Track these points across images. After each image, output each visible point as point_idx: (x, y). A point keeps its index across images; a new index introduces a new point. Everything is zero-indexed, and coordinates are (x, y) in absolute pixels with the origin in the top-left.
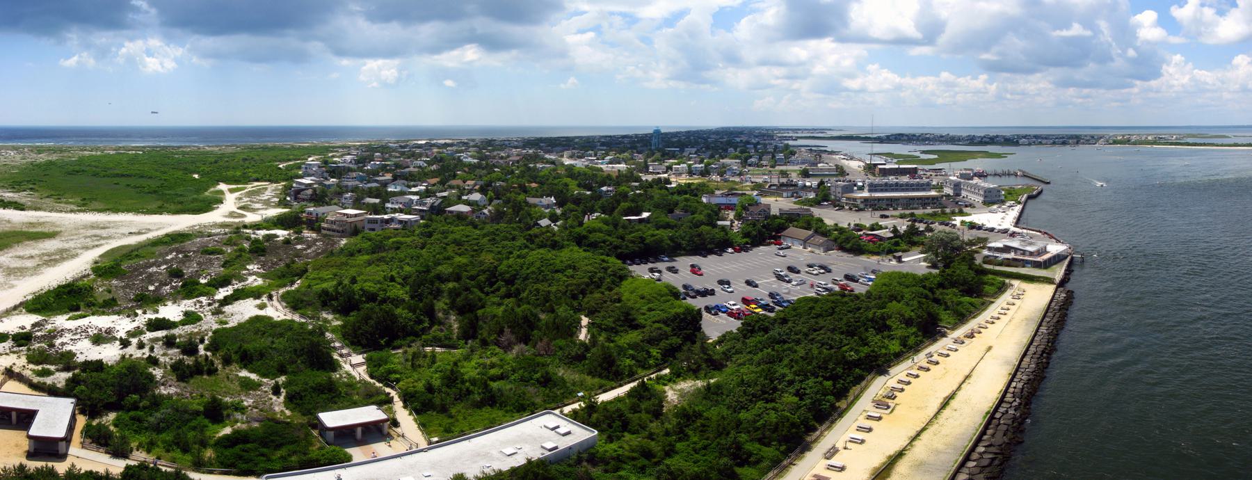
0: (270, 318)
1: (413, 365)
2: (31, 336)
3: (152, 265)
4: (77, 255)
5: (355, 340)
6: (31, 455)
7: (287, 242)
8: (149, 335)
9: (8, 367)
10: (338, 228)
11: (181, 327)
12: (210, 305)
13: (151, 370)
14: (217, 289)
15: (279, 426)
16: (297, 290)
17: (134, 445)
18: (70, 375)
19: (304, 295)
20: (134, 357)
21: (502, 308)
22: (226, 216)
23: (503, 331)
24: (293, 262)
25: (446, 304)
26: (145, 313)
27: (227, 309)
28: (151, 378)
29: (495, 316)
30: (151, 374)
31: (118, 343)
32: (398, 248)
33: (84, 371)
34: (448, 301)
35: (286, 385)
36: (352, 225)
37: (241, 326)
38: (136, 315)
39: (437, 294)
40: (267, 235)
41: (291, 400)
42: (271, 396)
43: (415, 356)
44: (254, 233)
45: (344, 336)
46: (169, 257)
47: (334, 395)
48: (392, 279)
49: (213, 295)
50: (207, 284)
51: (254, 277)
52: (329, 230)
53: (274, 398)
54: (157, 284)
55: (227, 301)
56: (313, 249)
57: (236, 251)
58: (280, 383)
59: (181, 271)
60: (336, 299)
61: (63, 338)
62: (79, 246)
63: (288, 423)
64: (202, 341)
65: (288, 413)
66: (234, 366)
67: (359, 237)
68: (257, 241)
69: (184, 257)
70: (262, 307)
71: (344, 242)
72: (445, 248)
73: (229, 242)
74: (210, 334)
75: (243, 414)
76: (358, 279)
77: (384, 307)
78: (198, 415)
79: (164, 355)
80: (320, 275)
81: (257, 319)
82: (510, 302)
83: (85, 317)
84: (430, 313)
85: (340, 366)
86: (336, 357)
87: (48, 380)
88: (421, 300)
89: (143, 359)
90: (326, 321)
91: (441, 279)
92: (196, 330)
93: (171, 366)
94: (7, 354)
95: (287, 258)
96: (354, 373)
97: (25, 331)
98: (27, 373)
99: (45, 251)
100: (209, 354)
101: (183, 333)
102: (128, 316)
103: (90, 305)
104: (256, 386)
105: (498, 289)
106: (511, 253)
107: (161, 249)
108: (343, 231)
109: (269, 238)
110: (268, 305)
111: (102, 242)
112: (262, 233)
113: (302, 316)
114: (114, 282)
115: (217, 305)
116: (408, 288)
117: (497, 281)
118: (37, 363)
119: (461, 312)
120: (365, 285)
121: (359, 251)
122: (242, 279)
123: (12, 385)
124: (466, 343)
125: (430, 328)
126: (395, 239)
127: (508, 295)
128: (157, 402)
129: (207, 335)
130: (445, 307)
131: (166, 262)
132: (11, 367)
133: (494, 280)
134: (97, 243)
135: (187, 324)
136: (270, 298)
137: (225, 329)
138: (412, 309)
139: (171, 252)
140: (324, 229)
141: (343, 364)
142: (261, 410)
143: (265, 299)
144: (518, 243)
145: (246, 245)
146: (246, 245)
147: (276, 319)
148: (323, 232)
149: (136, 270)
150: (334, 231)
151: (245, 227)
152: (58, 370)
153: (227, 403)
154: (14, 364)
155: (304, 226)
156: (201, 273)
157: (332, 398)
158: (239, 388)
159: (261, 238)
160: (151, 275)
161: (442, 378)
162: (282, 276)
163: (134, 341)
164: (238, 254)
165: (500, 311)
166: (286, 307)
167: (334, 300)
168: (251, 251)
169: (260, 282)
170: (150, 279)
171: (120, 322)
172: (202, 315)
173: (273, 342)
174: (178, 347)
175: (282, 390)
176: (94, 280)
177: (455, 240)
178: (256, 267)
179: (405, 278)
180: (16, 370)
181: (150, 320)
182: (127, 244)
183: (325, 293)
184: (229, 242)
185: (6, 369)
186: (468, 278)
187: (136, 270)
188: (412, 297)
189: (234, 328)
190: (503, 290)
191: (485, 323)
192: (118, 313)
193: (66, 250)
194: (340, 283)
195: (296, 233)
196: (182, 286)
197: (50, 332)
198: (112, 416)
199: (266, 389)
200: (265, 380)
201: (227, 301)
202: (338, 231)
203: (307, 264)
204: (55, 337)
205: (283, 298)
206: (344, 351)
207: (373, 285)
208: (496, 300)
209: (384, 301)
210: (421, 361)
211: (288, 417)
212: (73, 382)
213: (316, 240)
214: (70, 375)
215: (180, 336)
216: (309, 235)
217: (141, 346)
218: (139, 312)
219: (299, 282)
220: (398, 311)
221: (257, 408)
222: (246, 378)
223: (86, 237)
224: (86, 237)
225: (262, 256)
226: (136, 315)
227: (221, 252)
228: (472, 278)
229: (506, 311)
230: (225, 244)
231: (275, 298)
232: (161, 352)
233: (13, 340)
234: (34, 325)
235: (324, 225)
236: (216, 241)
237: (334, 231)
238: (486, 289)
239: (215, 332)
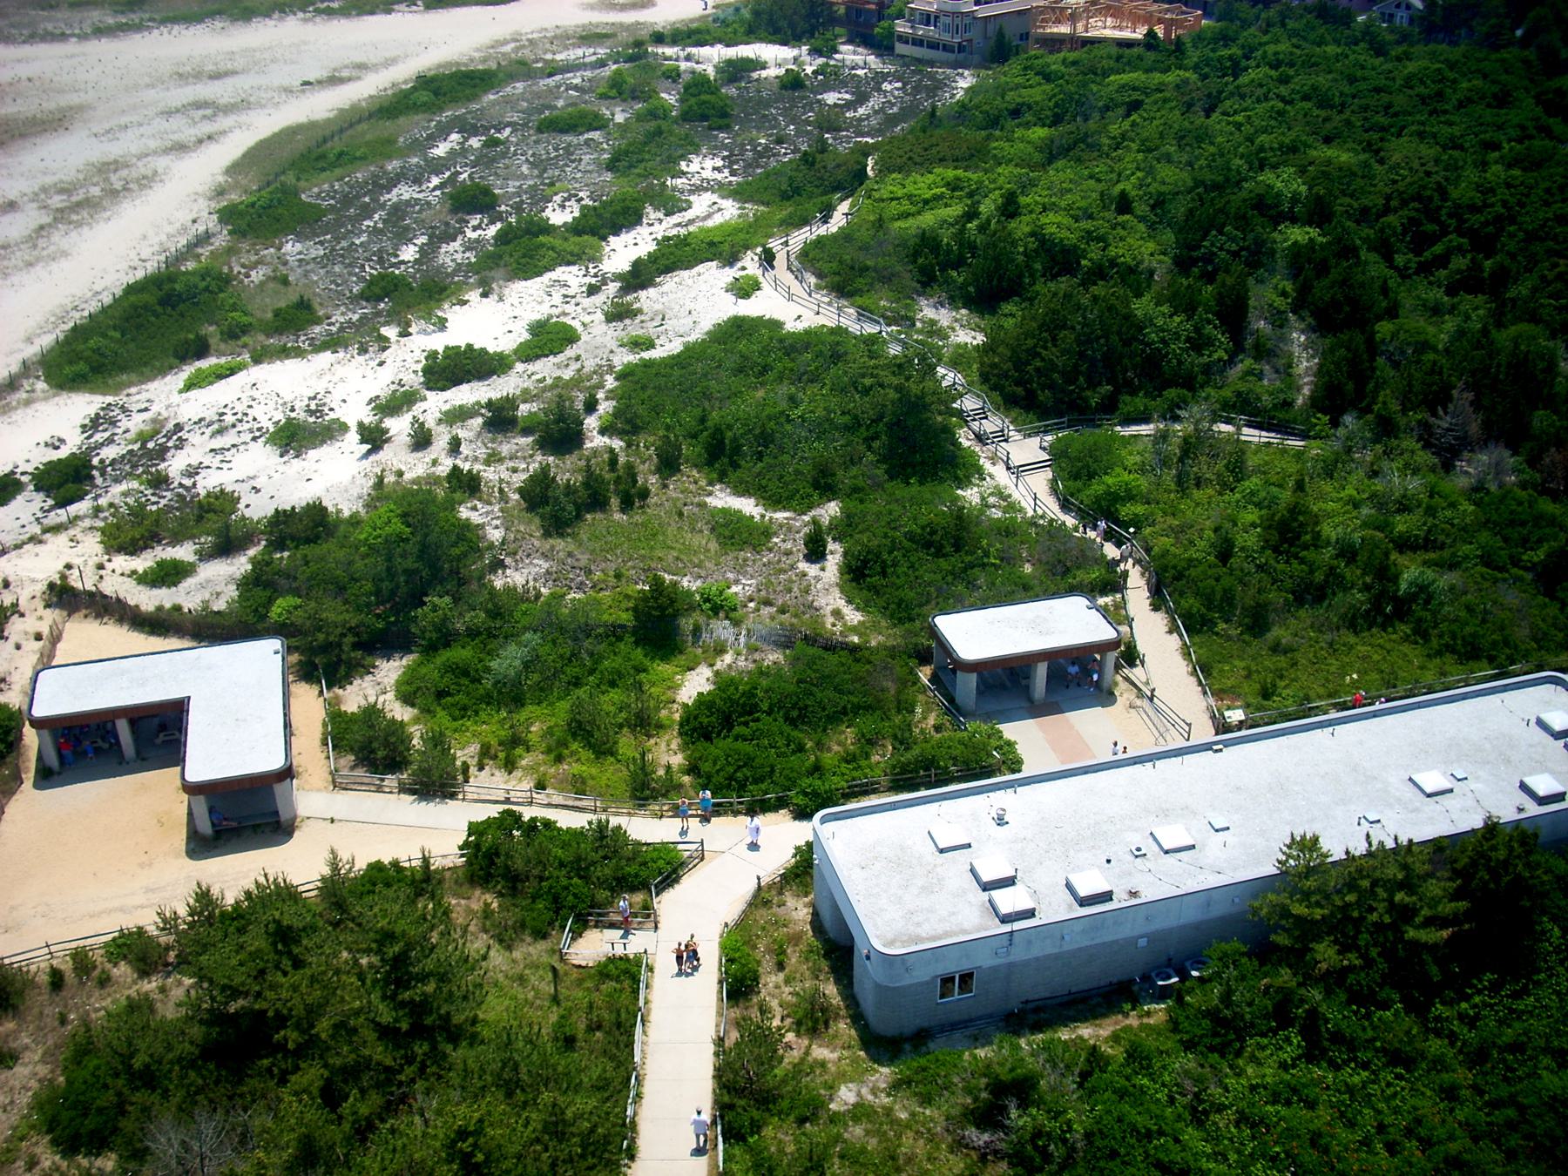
0: (776, 325)
1: (1180, 480)
2: (88, 465)
3: (393, 183)
4: (147, 181)
5: (1020, 390)
6: (202, 844)
7: (793, 82)
8: (434, 404)
9: (57, 579)
10: (946, 37)
11: (519, 367)
12: (592, 290)
13: (464, 513)
14: (604, 238)
15: (833, 659)
16: (845, 236)
17: (465, 753)
18: (240, 565)
19: (864, 248)
20: (408, 476)
21: (1450, 324)
22: (592, 7)
23: (1450, 399)
24: (823, 148)
25: (1284, 294)
26: (405, 334)
27: (647, 299)
28: (468, 535)
29: (1424, 346)
30: (467, 525)
31: (353, 436)
32: (1135, 106)
33: (278, 544)
34: (1288, 286)
35: (842, 529)
36: (992, 29)
37: (691, 353)
38: (384, 344)
39: (1257, 257)
40: (729, 62)
41: (857, 574)
42: (803, 566)
43: (1189, 448)
44: (688, 58)
45: (985, 378)
46: (441, 150)
47: (968, 559)
48: (1124, 205)
49: (596, 260)
50: (576, 228)
51: (708, 198)
52: (918, 42)
53: (812, 570)
54: (423, 240)
55: (640, 276)
56: (875, 102)
57: (639, 118)
58: (826, 521)
59: (487, 192)
60: (959, 264)
61: (187, 449)
62: (153, 144)
63: (854, 649)
64: (591, 407)
65: (853, 617)
66: (691, 476)
67: (1014, 67)
68: (698, 84)
69: (486, 145)
70: (745, 289)
71: (965, 81)
72: (1281, 113)
73: (618, 90)
74: (610, 382)
75: (737, 623)
76: (1023, 200)
77: (1098, 289)
78: (620, 639)
79: (493, 459)
80: (910, 189)
81: (738, 328)
82: (1476, 308)
83: (232, 371)
84: (1233, 315)
85: (980, 471)
86: (965, 439)
87: (187, 596)
88: (1210, 278)
89: (433, 480)
90: (933, 329)
91: (1270, 210)
92: (567, 374)
93: (520, 491)
94: (34, 540)
95: (798, 133)
96: (1020, 495)
97: (63, 453)
98: (114, 585)
99: (49, 180)
100: (617, 444)
101: (528, 384)
102: (363, 350)
103: (234, 334)
104: (766, 532)
105: (1442, 261)
106: (1495, 146)
107: (415, 126)
108: (961, 49)
109: (737, 71)
110: (764, 285)
111: (224, 122)
112: (711, 57)
113: (865, 313)
114: (291, 248)
115: (613, 288)
116: (1169, 236)
117: (1445, 232)
118: (133, 549)
119: (1325, 322)
120: (1044, 220)
121: (1016, 113)
122: (672, 205)
123: (85, 635)
124: (1335, 423)
125: (1231, 362)
126: (1125, 78)
127: (1467, 284)
128: (503, 610)
129: (601, 386)
130: (1279, 302)
131: (436, 166)
132: (64, 577)
133: (1431, 227)
134: (207, 128)
135: (538, 357)
136: (768, 259)
137: (647, 365)
138: (1188, 307)
139: (443, 133)
140: (904, 39)
141: (987, 466)
142: (783, 610)
143: (750, 264)
144: (1513, 116)
145: (670, 98)
146: (670, 98)
147: (791, 326)
148: (900, 48)
149: (352, 206)
150: (933, 45)
151: (659, 38)
152: (206, 556)
153: (689, 593)
154: (69, 567)
155: (838, 30)
156: (548, 191)
157: (965, 570)
158: (714, 546)
159: (711, 72)
160: (399, 210)
161: (1268, 525)
162: (791, 193)
163: (400, 426)
164: (651, 125)
165: (1442, 333)
166: (818, 288)
167: (956, 267)
168: (686, 117)
169: (730, 210)
170: (399, 223)
171: (340, 371)
172: (576, 324)
173: (793, 401)
174: (526, 432)
175: (832, 546)
176: (231, 251)
177: (1314, 88)
178: (709, 163)
179: (1159, 203)
180: (84, 581)
181: (432, 355)
182: (302, 119)
183: (927, 242)
184: (618, 90)
185: (51, 586)
186: (1350, 217)
187: (347, 201)
188: (1183, 264)
189: (675, 361)
190: (1460, 263)
191: (1396, 365)
192: (332, 343)
193: (116, 165)
194: (971, 215)
195: (816, 52)
196: (501, 238)
197: (143, 438)
198: (390, 670)
199: (789, 545)
200: (781, 516)
201: (640, 276)
202: (946, 48)
203: (865, 151)
204: (162, 452)
205: (810, 258)
206: (990, 425)
207: (1067, 221)
208: (1437, 295)
209: (1099, 273)
210: (1202, 467)
211: (854, 629)
212: (258, 583)
213: (880, 77)
214: (240, 565)
215: (527, 396)
216: (858, 59)
217: (421, 440)
218: (390, 332)
219: (844, 207)
220: (1141, 307)
221: (768, 603)
222: (725, 512)
223: (169, 113)
224: (169, 113)
225: (720, 129)
226: (384, 344)
227: (597, 123)
228: (1364, 216)
229: (1461, 333)
230: (604, 97)
231: (780, 261)
232: (482, 452)
233: (38, 489)
234: (94, 424)
235: (902, 27)
236: (576, 88)
237: (933, 45)
238: (1399, 260)
239: (624, 375)
